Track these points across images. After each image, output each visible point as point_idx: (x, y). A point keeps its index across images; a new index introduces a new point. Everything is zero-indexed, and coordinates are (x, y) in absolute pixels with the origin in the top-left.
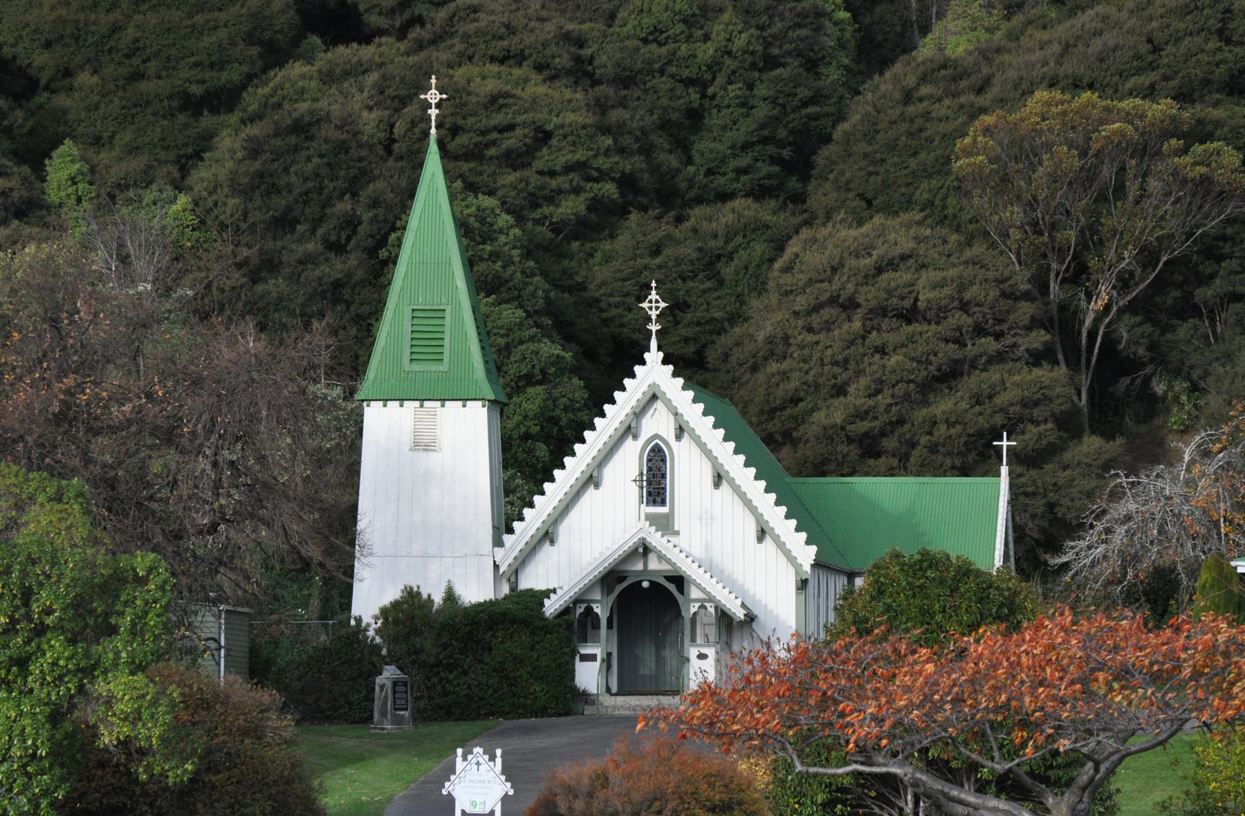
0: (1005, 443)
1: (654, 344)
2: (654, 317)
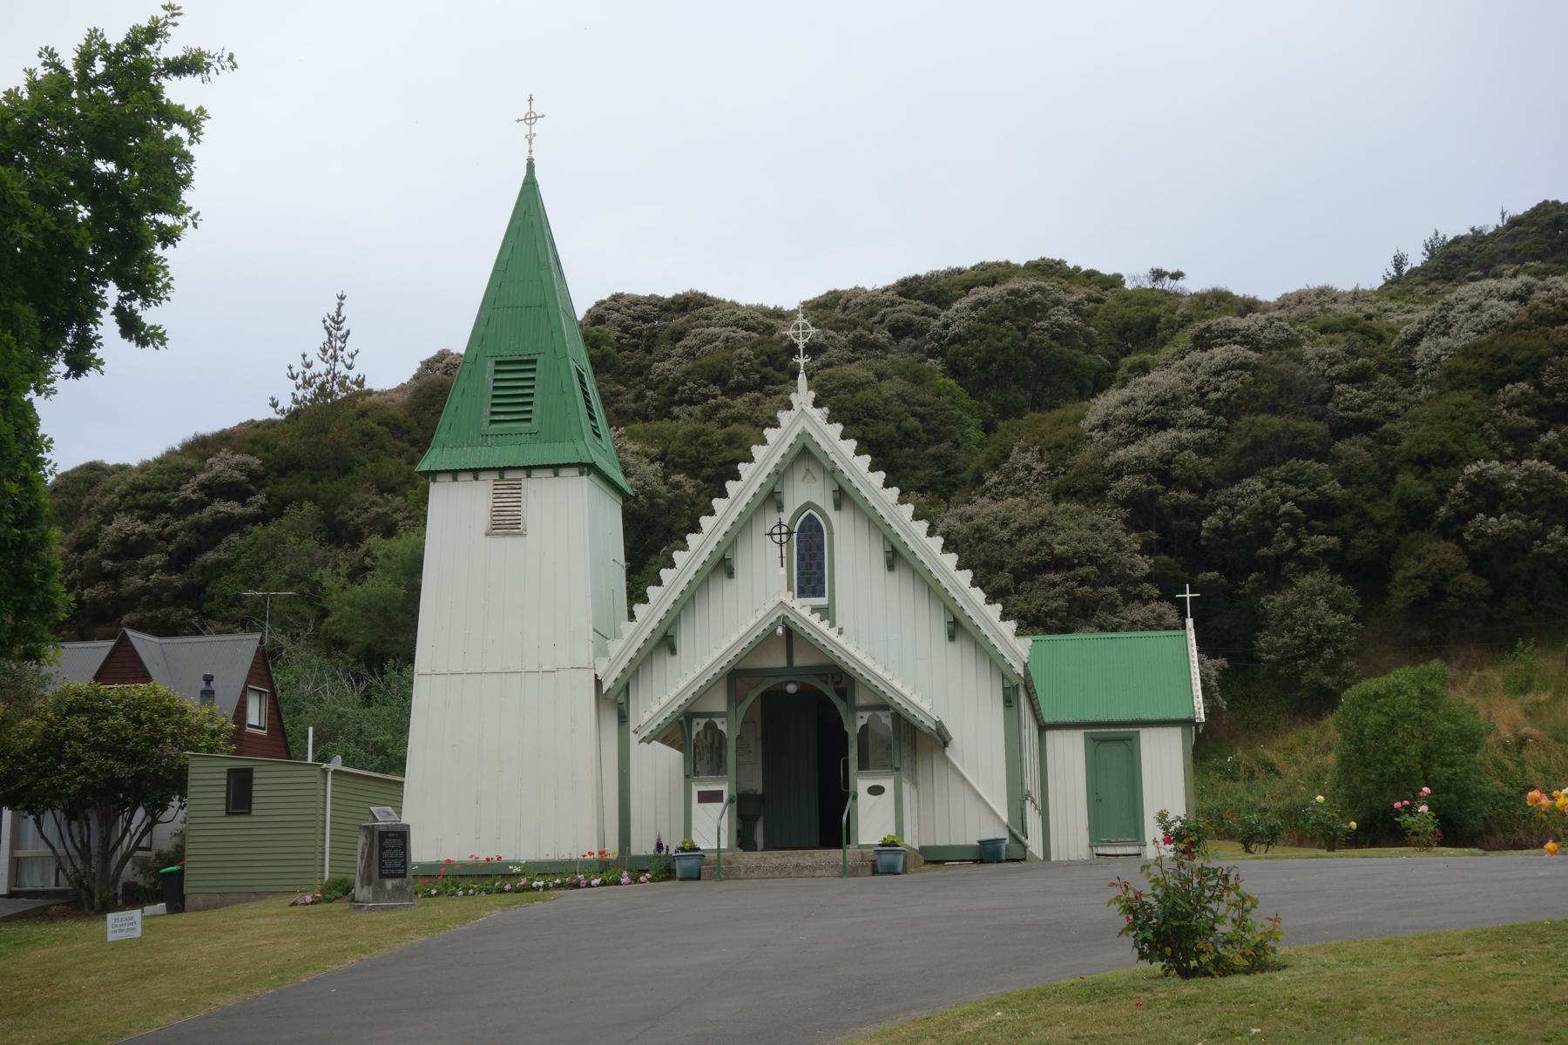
0: (1188, 595)
2: (801, 347)
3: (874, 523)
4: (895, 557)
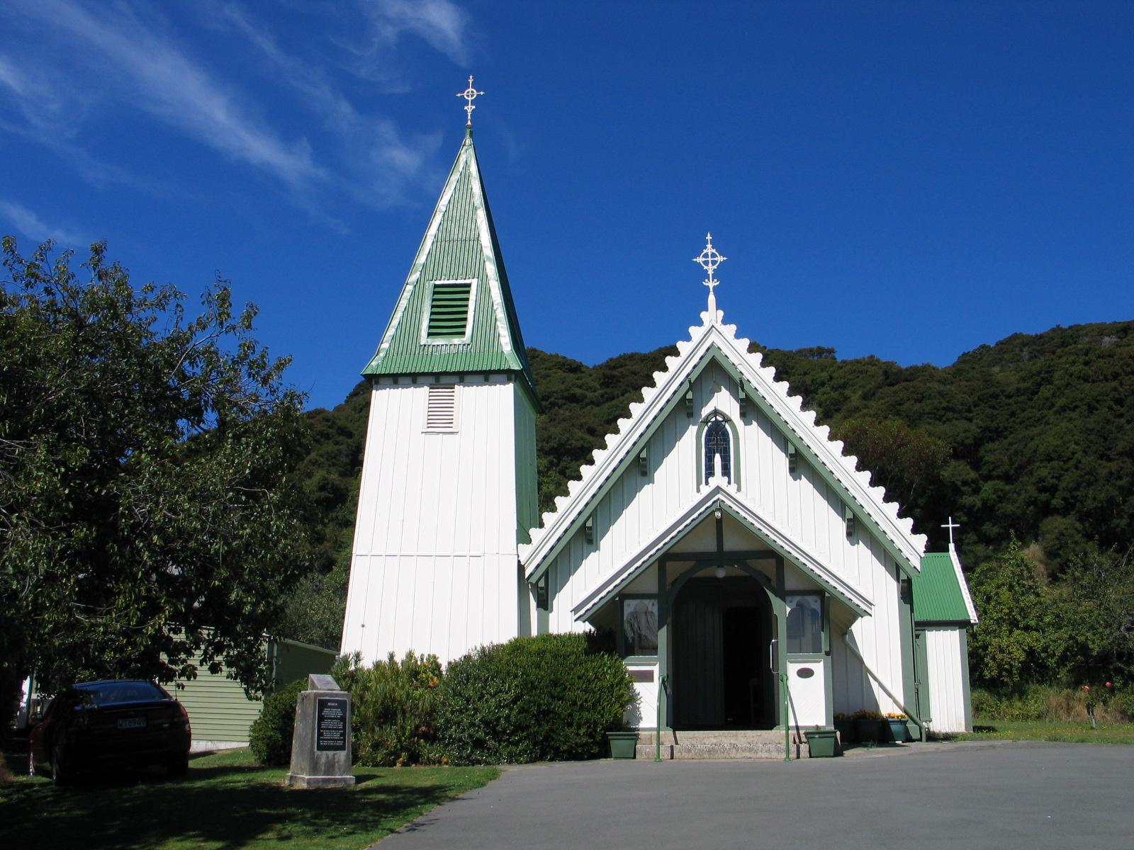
0: (951, 526)
1: (712, 299)
2: (710, 272)
3: (779, 433)
4: (801, 463)
